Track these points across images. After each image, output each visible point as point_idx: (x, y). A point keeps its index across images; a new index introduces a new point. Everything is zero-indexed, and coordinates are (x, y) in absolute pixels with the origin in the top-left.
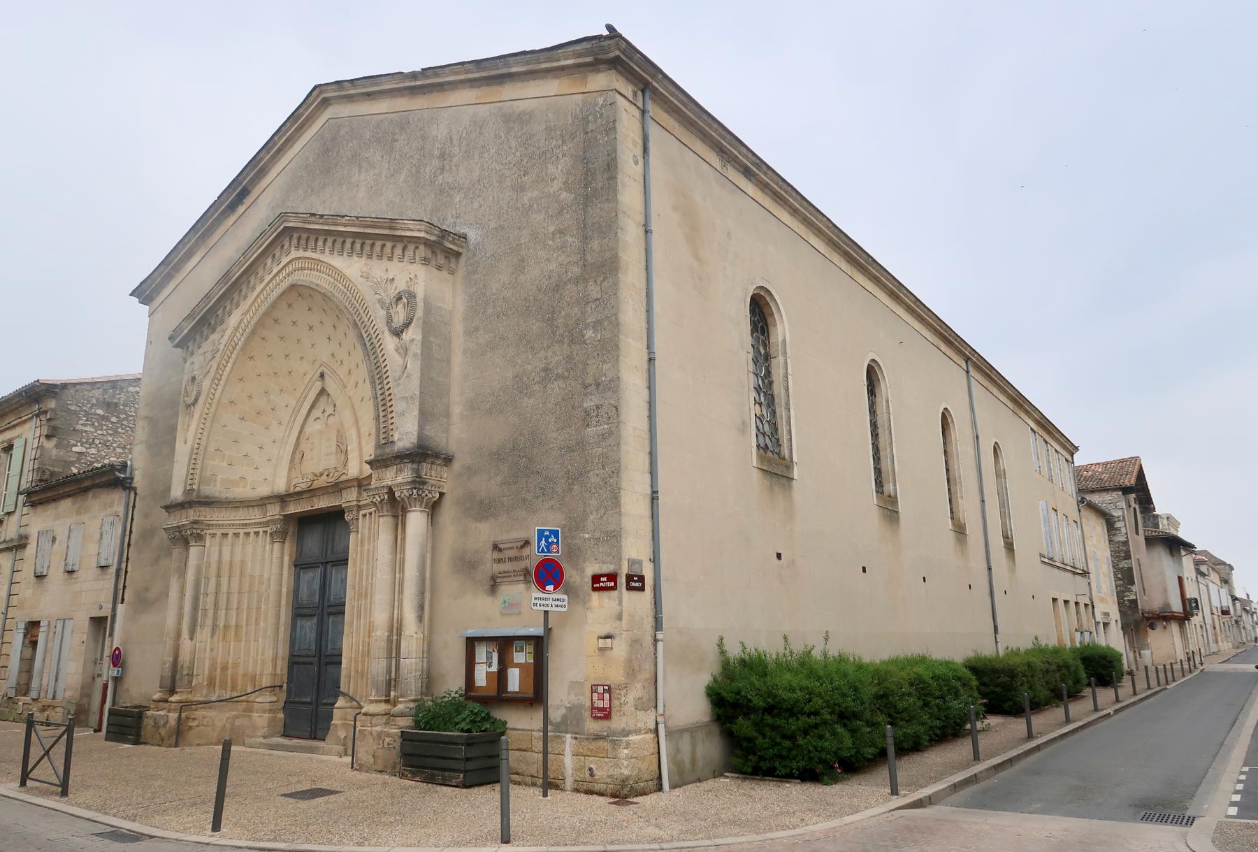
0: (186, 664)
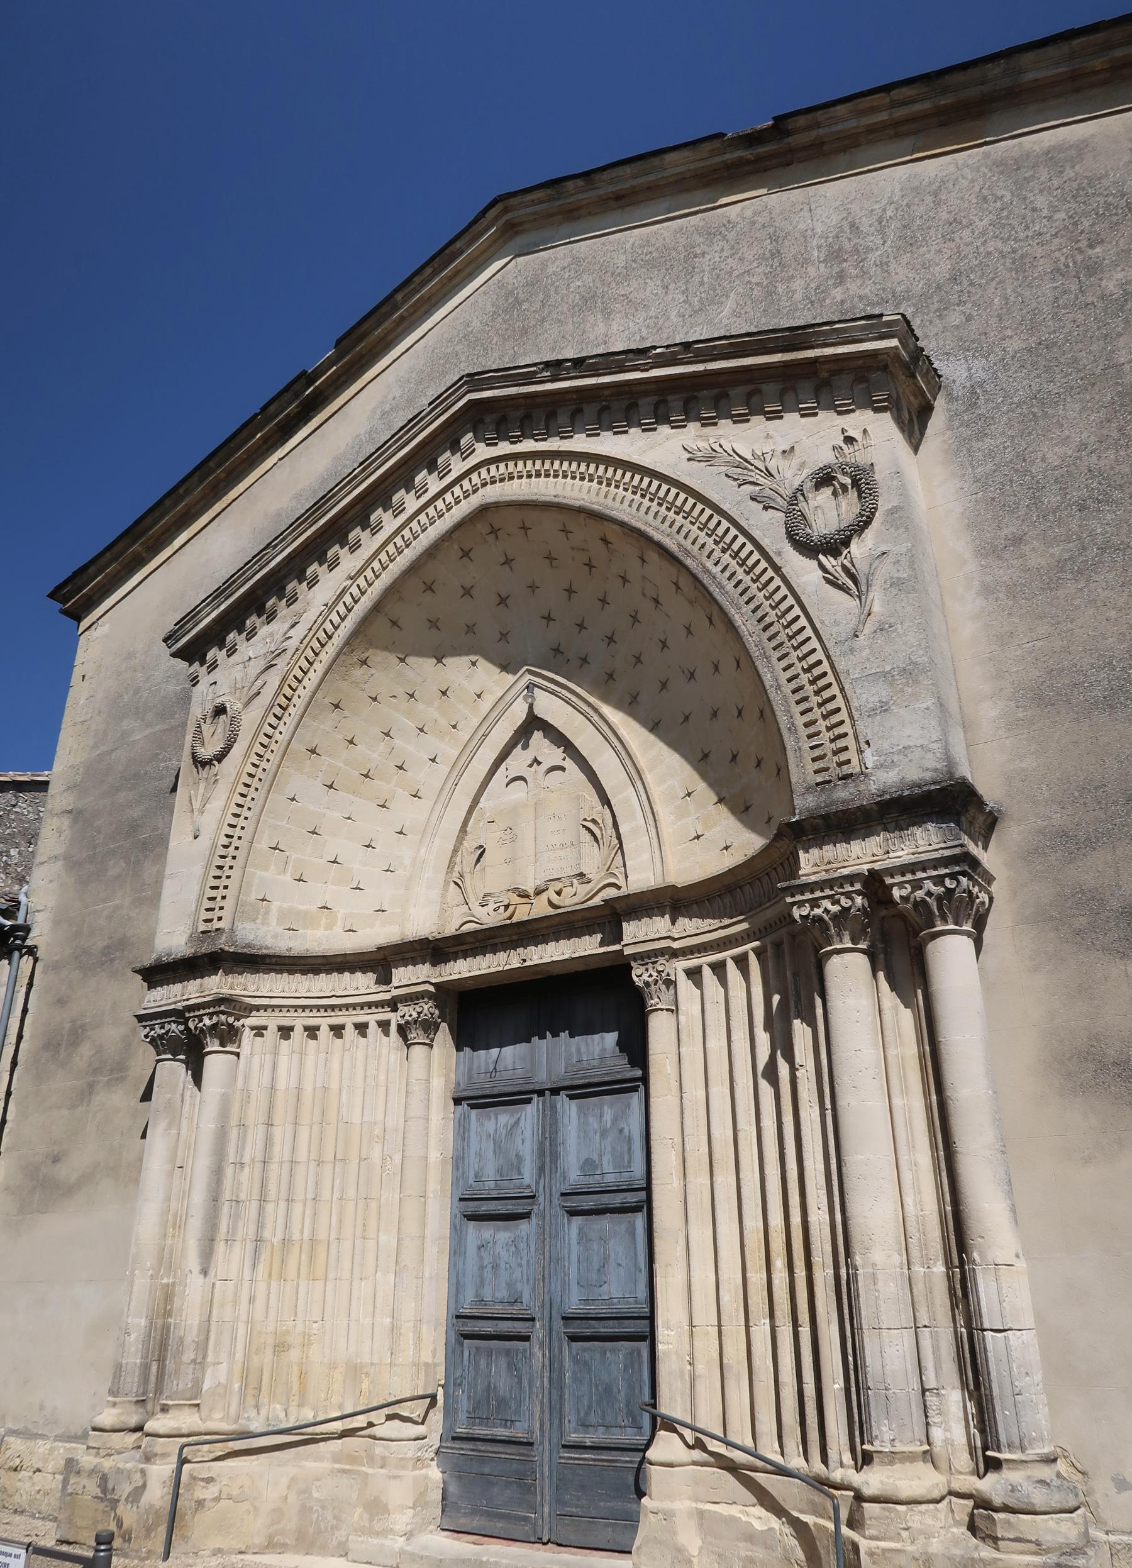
0: (191, 1336)
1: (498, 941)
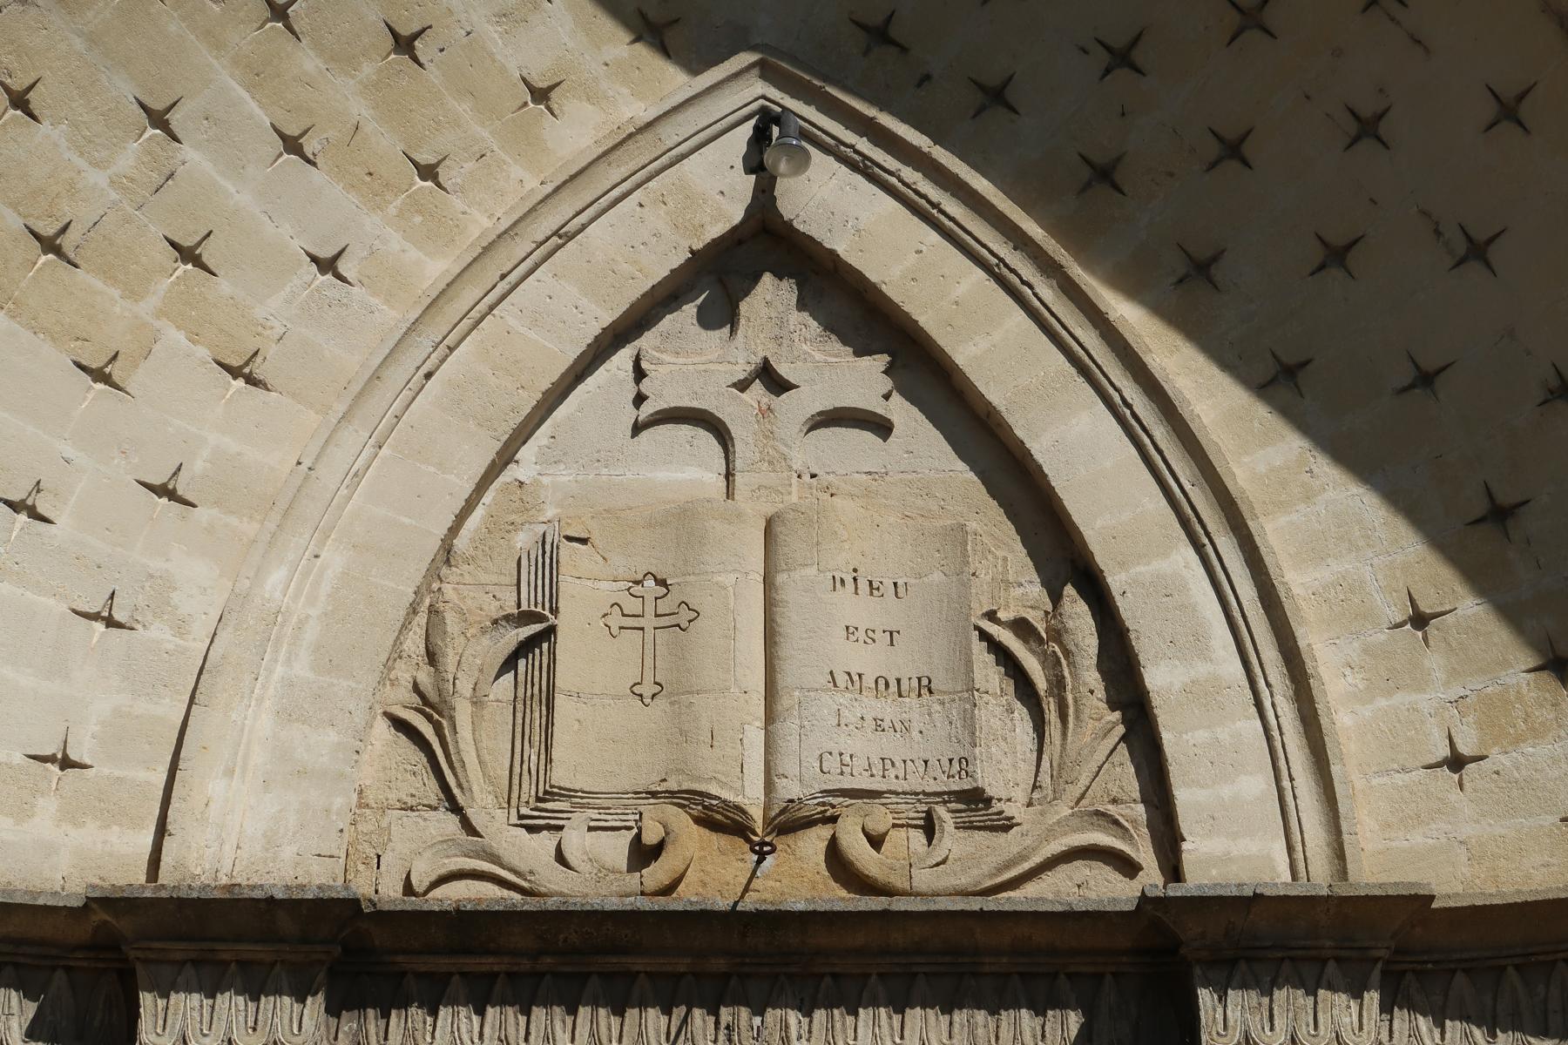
1: (638, 963)
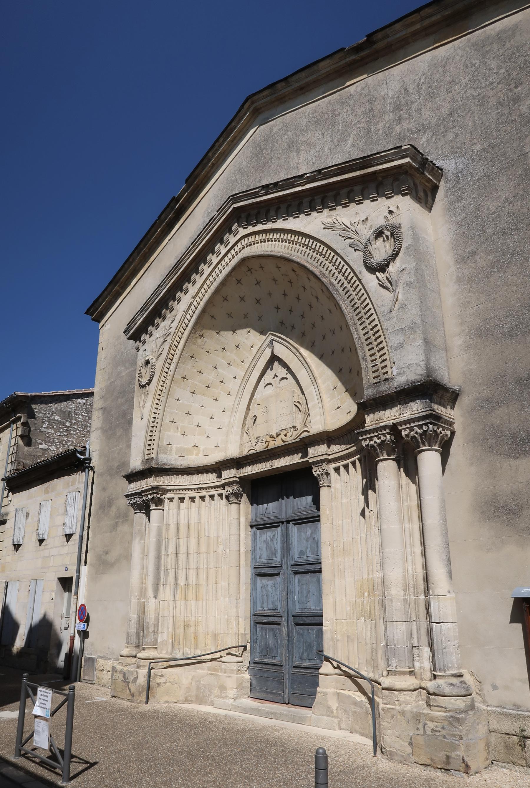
1: (261, 458)
